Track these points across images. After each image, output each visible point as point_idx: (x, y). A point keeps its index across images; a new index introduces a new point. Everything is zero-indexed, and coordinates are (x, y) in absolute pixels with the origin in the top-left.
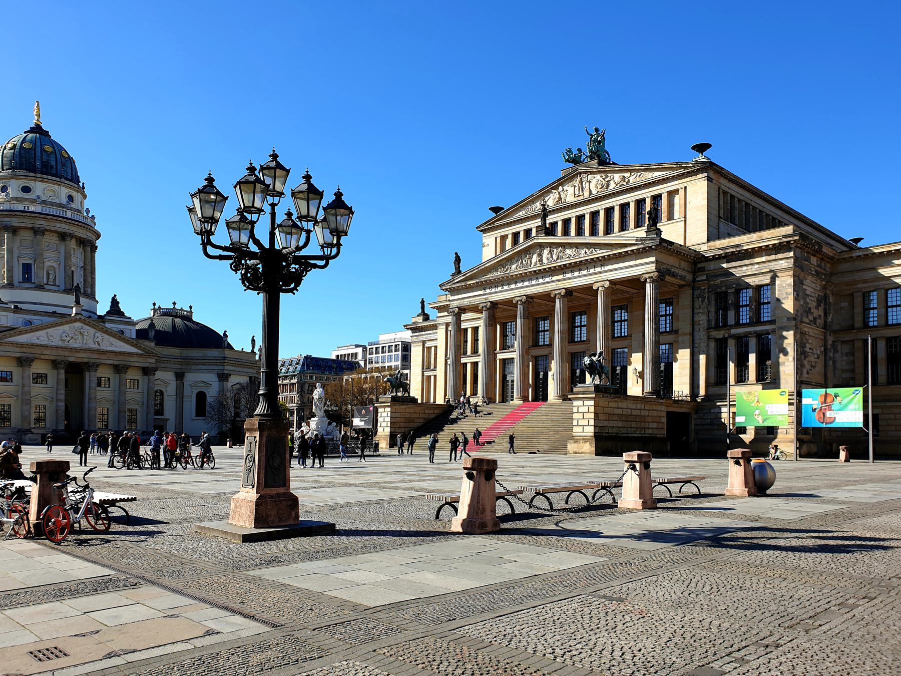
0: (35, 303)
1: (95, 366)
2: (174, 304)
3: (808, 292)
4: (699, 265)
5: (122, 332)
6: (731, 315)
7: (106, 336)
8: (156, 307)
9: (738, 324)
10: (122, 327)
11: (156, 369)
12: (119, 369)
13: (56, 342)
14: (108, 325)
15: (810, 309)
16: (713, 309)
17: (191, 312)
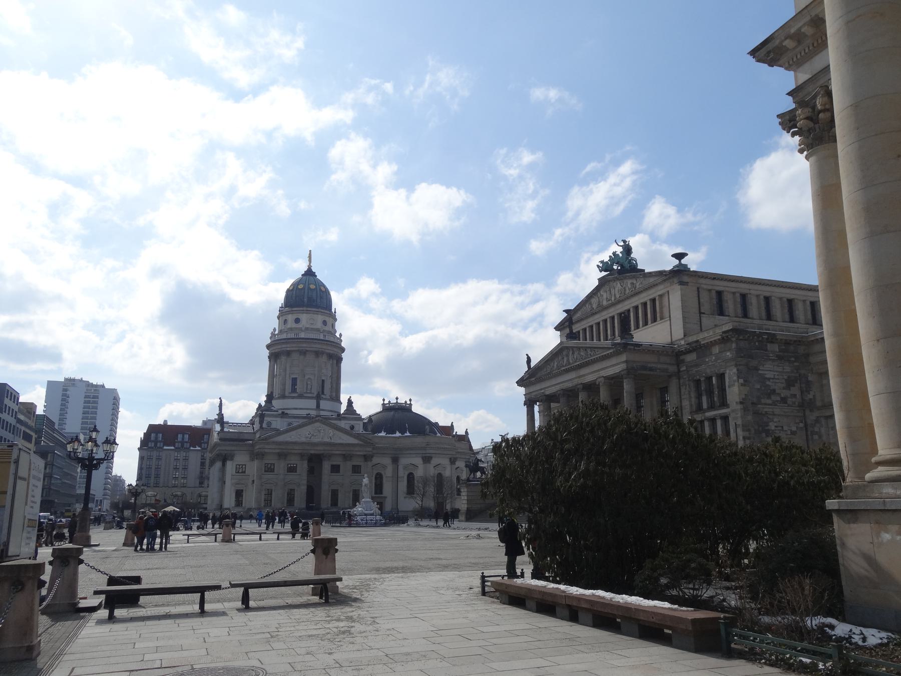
0: (296, 409)
1: (329, 456)
2: (397, 398)
3: (769, 375)
4: (682, 357)
5: (352, 428)
6: (704, 399)
7: (337, 432)
8: (386, 402)
9: (712, 407)
10: (352, 423)
11: (372, 457)
12: (346, 457)
13: (303, 440)
14: (343, 424)
15: (774, 390)
16: (693, 395)
17: (411, 404)
